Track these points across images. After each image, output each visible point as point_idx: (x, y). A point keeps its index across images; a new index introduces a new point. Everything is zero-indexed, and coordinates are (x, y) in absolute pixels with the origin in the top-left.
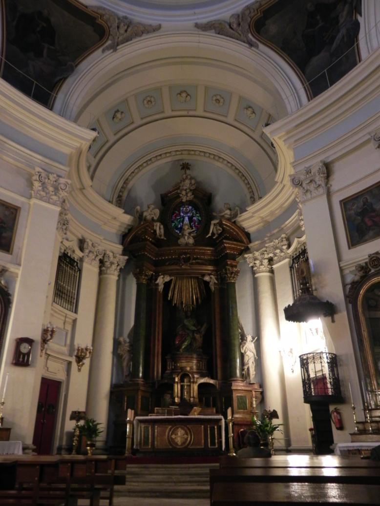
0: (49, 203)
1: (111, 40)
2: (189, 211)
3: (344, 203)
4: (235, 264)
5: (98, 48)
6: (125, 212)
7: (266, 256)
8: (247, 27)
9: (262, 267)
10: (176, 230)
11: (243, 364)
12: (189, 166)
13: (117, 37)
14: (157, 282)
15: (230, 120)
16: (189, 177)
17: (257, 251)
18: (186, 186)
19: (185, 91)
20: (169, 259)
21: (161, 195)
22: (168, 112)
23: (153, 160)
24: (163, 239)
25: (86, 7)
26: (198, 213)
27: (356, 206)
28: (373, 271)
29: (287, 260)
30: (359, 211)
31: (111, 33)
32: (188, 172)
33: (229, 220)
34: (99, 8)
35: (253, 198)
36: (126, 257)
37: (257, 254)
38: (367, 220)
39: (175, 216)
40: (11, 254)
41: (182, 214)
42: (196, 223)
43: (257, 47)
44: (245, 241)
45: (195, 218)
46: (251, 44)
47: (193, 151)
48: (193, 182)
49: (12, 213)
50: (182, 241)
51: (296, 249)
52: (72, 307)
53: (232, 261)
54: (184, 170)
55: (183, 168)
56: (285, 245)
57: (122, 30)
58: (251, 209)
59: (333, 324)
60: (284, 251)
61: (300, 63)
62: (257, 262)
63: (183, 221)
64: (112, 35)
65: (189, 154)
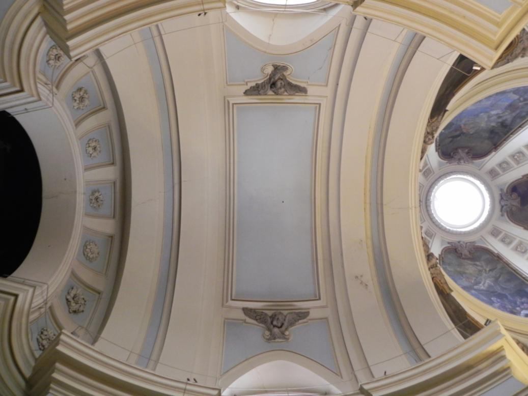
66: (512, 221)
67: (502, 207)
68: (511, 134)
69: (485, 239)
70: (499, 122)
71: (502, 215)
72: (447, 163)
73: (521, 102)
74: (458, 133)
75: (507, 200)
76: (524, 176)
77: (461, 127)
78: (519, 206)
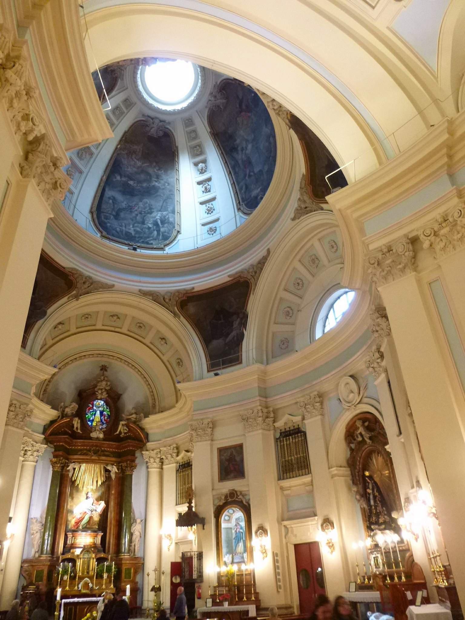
3: (221, 451)
5: (66, 296)
6: (52, 408)
7: (159, 456)
8: (175, 303)
11: (130, 541)
14: (68, 469)
15: (147, 342)
16: (106, 379)
17: (153, 450)
20: (81, 450)
22: (99, 326)
23: (78, 359)
25: (64, 268)
28: (230, 500)
29: (175, 465)
31: (78, 286)
32: (105, 373)
33: (135, 423)
34: (73, 269)
36: (46, 446)
37: (153, 454)
38: (231, 465)
39: (89, 409)
41: (95, 408)
42: (106, 418)
43: (179, 318)
46: (175, 315)
48: (109, 383)
50: (94, 435)
51: (183, 458)
55: (101, 370)
57: (86, 286)
58: (152, 418)
61: (206, 340)
62: (152, 460)
63: (95, 414)
64: (77, 288)
66: (135, 123)
67: (152, 119)
68: (222, 153)
69: (122, 91)
70: (238, 147)
71: (143, 115)
72: (216, 83)
73: (250, 172)
74: (244, 107)
75: (158, 125)
76: (177, 147)
77: (249, 112)
78: (149, 134)
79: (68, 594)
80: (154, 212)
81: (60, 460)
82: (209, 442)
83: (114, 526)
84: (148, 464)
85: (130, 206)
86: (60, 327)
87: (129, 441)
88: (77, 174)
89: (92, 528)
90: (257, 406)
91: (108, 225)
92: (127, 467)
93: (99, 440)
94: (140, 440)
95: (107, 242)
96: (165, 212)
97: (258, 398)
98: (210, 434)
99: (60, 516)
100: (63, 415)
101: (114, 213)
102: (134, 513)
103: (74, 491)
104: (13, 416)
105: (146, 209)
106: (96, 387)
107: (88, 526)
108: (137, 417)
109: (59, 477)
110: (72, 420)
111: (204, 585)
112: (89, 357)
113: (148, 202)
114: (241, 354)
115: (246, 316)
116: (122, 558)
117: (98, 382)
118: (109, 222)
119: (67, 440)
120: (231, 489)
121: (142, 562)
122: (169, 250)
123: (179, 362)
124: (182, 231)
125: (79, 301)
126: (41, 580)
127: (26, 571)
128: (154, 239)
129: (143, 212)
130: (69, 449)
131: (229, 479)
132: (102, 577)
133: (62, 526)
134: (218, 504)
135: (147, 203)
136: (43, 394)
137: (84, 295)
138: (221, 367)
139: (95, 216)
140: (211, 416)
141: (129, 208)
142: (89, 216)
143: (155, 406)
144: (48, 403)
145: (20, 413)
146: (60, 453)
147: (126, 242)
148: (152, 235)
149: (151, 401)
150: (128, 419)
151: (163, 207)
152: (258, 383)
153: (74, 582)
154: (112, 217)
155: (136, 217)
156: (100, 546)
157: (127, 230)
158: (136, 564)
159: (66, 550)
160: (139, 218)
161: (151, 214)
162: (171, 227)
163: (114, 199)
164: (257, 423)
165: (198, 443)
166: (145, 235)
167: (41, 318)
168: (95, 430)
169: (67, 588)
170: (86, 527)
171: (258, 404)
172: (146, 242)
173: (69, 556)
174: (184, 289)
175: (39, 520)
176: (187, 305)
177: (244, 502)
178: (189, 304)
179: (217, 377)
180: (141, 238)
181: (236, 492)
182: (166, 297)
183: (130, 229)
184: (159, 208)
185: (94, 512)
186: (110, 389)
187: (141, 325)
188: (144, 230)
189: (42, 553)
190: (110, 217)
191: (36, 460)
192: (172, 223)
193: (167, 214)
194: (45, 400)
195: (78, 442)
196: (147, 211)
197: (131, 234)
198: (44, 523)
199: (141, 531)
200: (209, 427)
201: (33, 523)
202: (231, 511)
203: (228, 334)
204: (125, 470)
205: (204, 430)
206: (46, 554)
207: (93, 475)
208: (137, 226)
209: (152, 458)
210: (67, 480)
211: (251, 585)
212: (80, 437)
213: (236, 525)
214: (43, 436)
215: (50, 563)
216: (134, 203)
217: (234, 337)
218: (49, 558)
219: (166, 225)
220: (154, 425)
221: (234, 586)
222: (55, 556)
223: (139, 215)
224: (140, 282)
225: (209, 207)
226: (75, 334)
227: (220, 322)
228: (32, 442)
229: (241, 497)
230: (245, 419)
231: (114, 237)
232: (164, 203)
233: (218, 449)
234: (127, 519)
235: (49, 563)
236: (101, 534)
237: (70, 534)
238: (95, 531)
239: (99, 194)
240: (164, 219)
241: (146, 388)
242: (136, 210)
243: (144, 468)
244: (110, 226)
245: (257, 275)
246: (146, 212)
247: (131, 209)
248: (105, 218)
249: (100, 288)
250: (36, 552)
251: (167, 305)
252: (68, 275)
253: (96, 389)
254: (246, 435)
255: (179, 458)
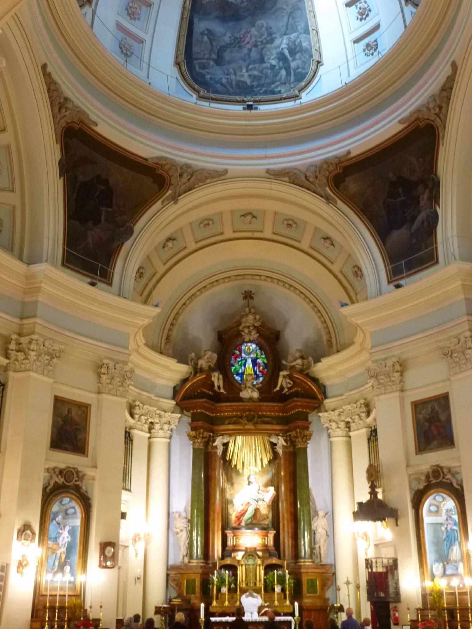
0: (116, 395)
1: (171, 190)
2: (252, 351)
3: (417, 406)
4: (306, 425)
7: (343, 418)
8: (325, 181)
9: (338, 430)
10: (237, 375)
11: (313, 542)
12: (253, 295)
13: (179, 187)
14: (215, 444)
15: (304, 245)
16: (253, 310)
17: (333, 410)
18: (249, 323)
19: (251, 213)
20: (230, 417)
21: (218, 332)
23: (208, 286)
24: (222, 393)
25: (146, 160)
26: (263, 353)
27: (425, 410)
28: (434, 481)
29: (364, 430)
30: (427, 417)
31: (172, 182)
35: (330, 341)
36: (179, 415)
37: (333, 415)
39: (236, 358)
40: (87, 456)
41: (243, 355)
42: (261, 368)
44: (320, 397)
45: (259, 361)
46: (328, 199)
47: (258, 275)
48: (258, 317)
49: (84, 411)
50: (245, 394)
52: (124, 484)
53: (304, 422)
54: (247, 301)
55: (245, 298)
56: (363, 412)
57: (184, 180)
58: (325, 362)
59: (397, 528)
60: (362, 418)
64: (173, 184)
65: (253, 279)
79: (228, 611)
80: (276, 38)
81: (199, 434)
82: (397, 394)
83: (288, 522)
84: (329, 431)
85: (237, 38)
86: (170, 244)
87: (295, 399)
88: (144, 8)
89: (261, 524)
90: (465, 331)
91: (208, 77)
92: (296, 437)
93: (254, 401)
94: (312, 396)
95: (205, 105)
96: (293, 35)
97: (465, 318)
98: (397, 382)
99: (211, 508)
100: (197, 370)
101: (214, 56)
102: (314, 503)
103: (233, 475)
104: (107, 381)
105: (264, 37)
106: (240, 324)
107: (254, 522)
108: (303, 363)
109: (202, 457)
110: (209, 377)
111: (402, 606)
112: (224, 282)
113: (265, 24)
114: (436, 248)
115: (436, 184)
116: (301, 566)
117: (242, 317)
118: (208, 73)
119: (207, 405)
120: (435, 464)
121: (333, 571)
122: (307, 97)
123: (356, 272)
124: (325, 60)
125: (178, 205)
126: (194, 593)
127: (174, 580)
128: (282, 84)
129: (259, 43)
130: (212, 417)
131: (431, 449)
132: (273, 590)
133: (216, 522)
134: (416, 489)
135: (263, 26)
136: (166, 344)
137: (185, 192)
138: (404, 275)
139: (184, 68)
140: (397, 352)
141: (237, 41)
142: (175, 72)
143: (331, 343)
144: (173, 356)
145: (116, 375)
146: (200, 423)
147: (238, 98)
148: (278, 78)
149: (325, 338)
150: (293, 367)
151: (289, 27)
152: (464, 293)
153: (235, 596)
154: (212, 63)
155: (249, 54)
156: (273, 548)
157: (238, 78)
158: (323, 573)
159: (226, 553)
160: (254, 54)
161: (272, 43)
162: (307, 56)
163: (210, 33)
164: (467, 359)
165: (381, 397)
166: (267, 80)
167: (127, 239)
168: (246, 387)
169: (227, 603)
170: (251, 523)
171: (467, 327)
172: (270, 91)
173: (228, 561)
174: (336, 157)
175: (184, 515)
176: (344, 181)
177: (455, 485)
178: (348, 179)
179: (400, 290)
180: (263, 86)
181: (442, 468)
182: (308, 174)
183: (242, 76)
184: (283, 30)
185: (260, 502)
186: (263, 325)
187: (290, 223)
188: (264, 72)
189: (191, 557)
190: (209, 64)
191: (168, 435)
192: (307, 49)
193: (298, 37)
194: (171, 351)
195: (223, 407)
196: (265, 39)
197: (246, 83)
198: (189, 518)
199: (326, 527)
200: (395, 370)
201: (175, 519)
202: (439, 498)
203: (414, 218)
204: (295, 441)
205: (388, 375)
206: (197, 558)
207: (254, 452)
208: (252, 69)
209: (334, 421)
210: (215, 461)
211: (467, 609)
212: (228, 400)
213: (447, 519)
214: (174, 402)
215: (202, 571)
216: (243, 32)
217: (423, 222)
218: (202, 564)
219: (298, 56)
220: (331, 373)
221: (444, 609)
222: (210, 562)
223: (254, 49)
224: (266, 157)
225: (360, 8)
226: (196, 251)
227: (398, 200)
228: (158, 412)
229: (449, 476)
230: (448, 354)
231: (219, 93)
232: (290, 19)
233: (412, 403)
234: (303, 511)
235: (200, 571)
236: (272, 534)
237: (230, 533)
238: (263, 529)
239: (185, 32)
240: (294, 47)
241: (315, 318)
242: (248, 43)
243: (325, 436)
244: (211, 78)
245: (443, 111)
246: (265, 41)
247: (239, 42)
248: (200, 68)
249: (207, 178)
250: (184, 556)
251: (313, 186)
252: (155, 169)
253: (241, 328)
254: (452, 379)
255: (369, 420)
